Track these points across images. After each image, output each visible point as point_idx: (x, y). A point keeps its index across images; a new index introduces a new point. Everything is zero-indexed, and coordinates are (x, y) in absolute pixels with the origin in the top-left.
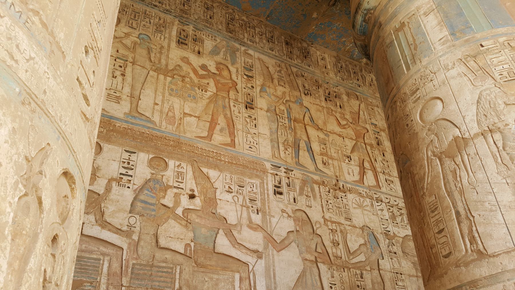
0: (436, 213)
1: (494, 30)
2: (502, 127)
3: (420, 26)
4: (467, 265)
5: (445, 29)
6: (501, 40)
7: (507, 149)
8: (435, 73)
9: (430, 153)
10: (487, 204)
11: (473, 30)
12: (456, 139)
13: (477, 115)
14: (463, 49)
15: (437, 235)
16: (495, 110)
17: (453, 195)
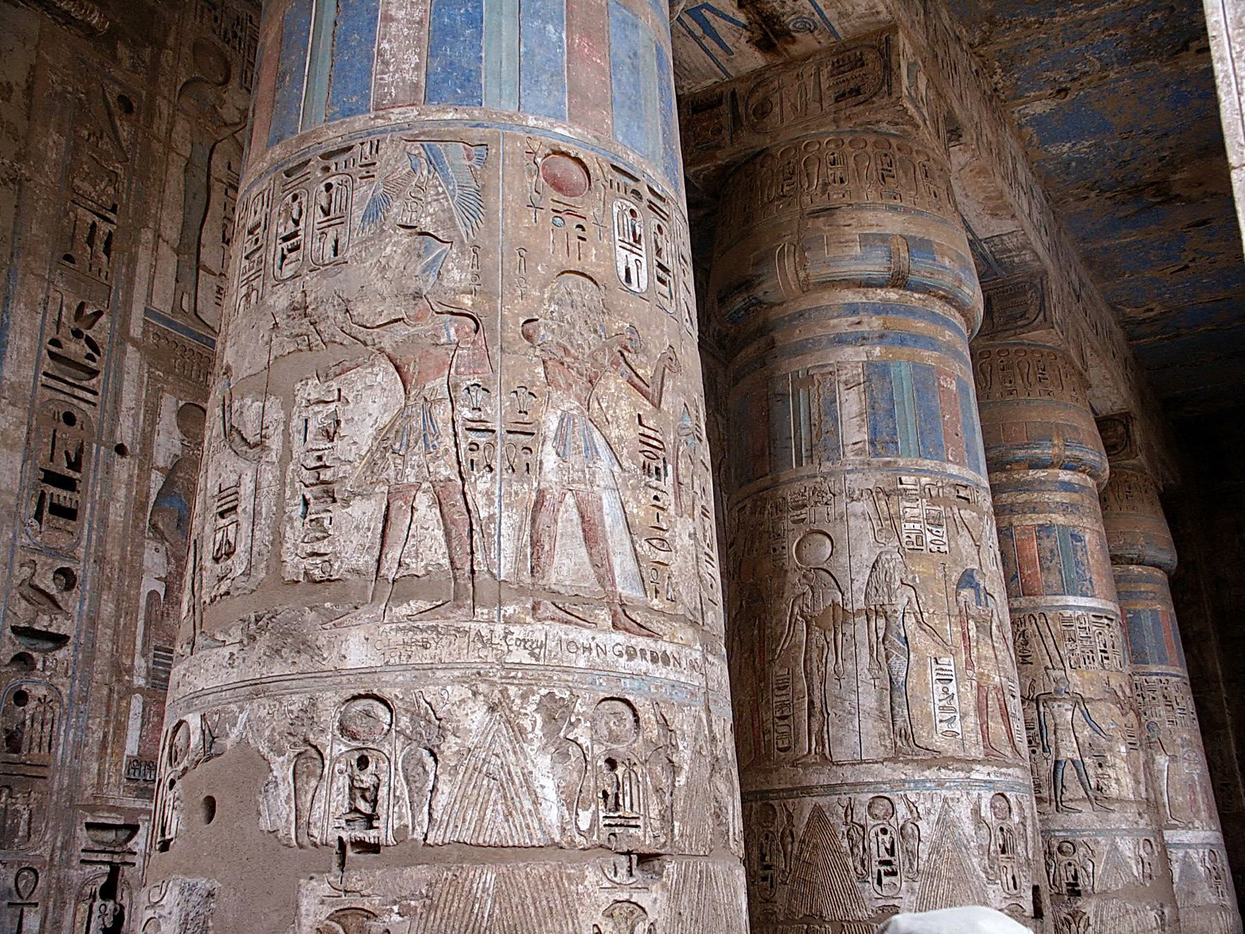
0: (784, 692)
2: (889, 613)
3: (835, 401)
4: (806, 766)
5: (865, 429)
6: (924, 480)
7: (887, 642)
8: (834, 495)
9: (796, 610)
10: (847, 703)
11: (897, 449)
12: (835, 605)
13: (868, 584)
14: (879, 477)
15: (777, 720)
16: (889, 587)
17: (812, 678)
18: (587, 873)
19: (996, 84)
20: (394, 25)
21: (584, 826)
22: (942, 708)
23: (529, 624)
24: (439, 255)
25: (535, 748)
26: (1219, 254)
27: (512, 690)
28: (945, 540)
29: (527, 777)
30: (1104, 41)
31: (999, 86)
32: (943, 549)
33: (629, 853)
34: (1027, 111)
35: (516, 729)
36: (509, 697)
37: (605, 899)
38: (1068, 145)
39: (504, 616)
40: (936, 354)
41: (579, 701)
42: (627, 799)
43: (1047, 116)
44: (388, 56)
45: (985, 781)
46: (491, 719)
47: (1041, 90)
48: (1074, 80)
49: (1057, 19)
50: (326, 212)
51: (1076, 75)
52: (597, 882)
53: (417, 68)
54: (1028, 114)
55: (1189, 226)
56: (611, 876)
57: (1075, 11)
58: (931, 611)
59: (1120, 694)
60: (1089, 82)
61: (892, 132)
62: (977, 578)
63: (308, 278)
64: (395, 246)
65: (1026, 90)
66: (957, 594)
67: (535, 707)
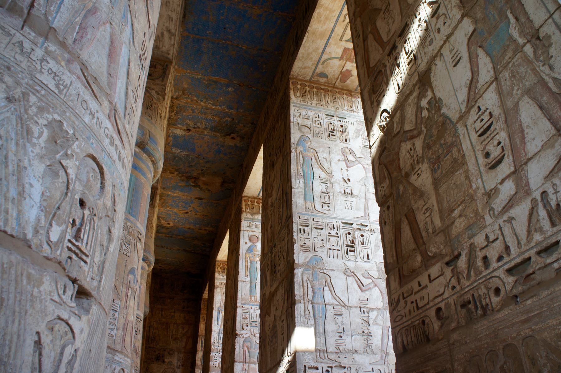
1: (129, 216)
18: (44, 280)
19: (171, 116)
21: (54, 237)
22: (110, 323)
23: (62, 66)
25: (35, 151)
26: (199, 212)
27: (33, 99)
28: (129, 251)
29: (20, 170)
30: (210, 119)
31: (172, 117)
32: (128, 254)
33: (74, 281)
34: (174, 131)
35: (25, 127)
36: (28, 101)
37: (53, 310)
38: (179, 151)
39: (46, 48)
40: (145, 179)
41: (77, 143)
42: (86, 236)
43: (179, 137)
45: (119, 361)
46: (6, 106)
47: (183, 126)
48: (194, 128)
49: (202, 103)
51: (196, 127)
52: (50, 292)
54: (174, 133)
55: (197, 198)
56: (61, 292)
57: (208, 103)
58: (117, 278)
59: (137, 349)
60: (199, 131)
61: (155, 96)
62: (136, 272)
65: (179, 124)
66: (128, 275)
67: (45, 122)
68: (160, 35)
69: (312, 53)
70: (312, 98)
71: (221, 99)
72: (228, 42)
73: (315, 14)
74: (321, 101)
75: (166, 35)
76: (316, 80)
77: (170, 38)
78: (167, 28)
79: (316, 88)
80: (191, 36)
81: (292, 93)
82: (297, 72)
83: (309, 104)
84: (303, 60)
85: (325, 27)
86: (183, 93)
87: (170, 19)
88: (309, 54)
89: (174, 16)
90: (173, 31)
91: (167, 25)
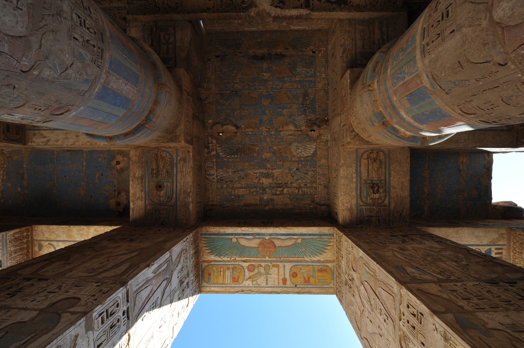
20: (124, 85)
24: (57, 70)
44: (119, 80)
49: (2, 172)
50: (88, 41)
53: (112, 87)
57: (3, 176)
63: (70, 23)
64: (67, 58)
68: (44, 136)
69: (55, 234)
70: (14, 246)
71: (10, 185)
72: (56, 180)
73: (82, 227)
74: (15, 253)
75: (45, 140)
76: (35, 244)
77: (43, 142)
78: (50, 139)
79: (28, 246)
80: (55, 157)
81: (17, 230)
82: (38, 229)
83: (8, 246)
84: (48, 230)
85: (76, 236)
86: (8, 157)
87: (57, 141)
88: (54, 232)
89: (60, 143)
90: (49, 143)
91: (53, 139)
